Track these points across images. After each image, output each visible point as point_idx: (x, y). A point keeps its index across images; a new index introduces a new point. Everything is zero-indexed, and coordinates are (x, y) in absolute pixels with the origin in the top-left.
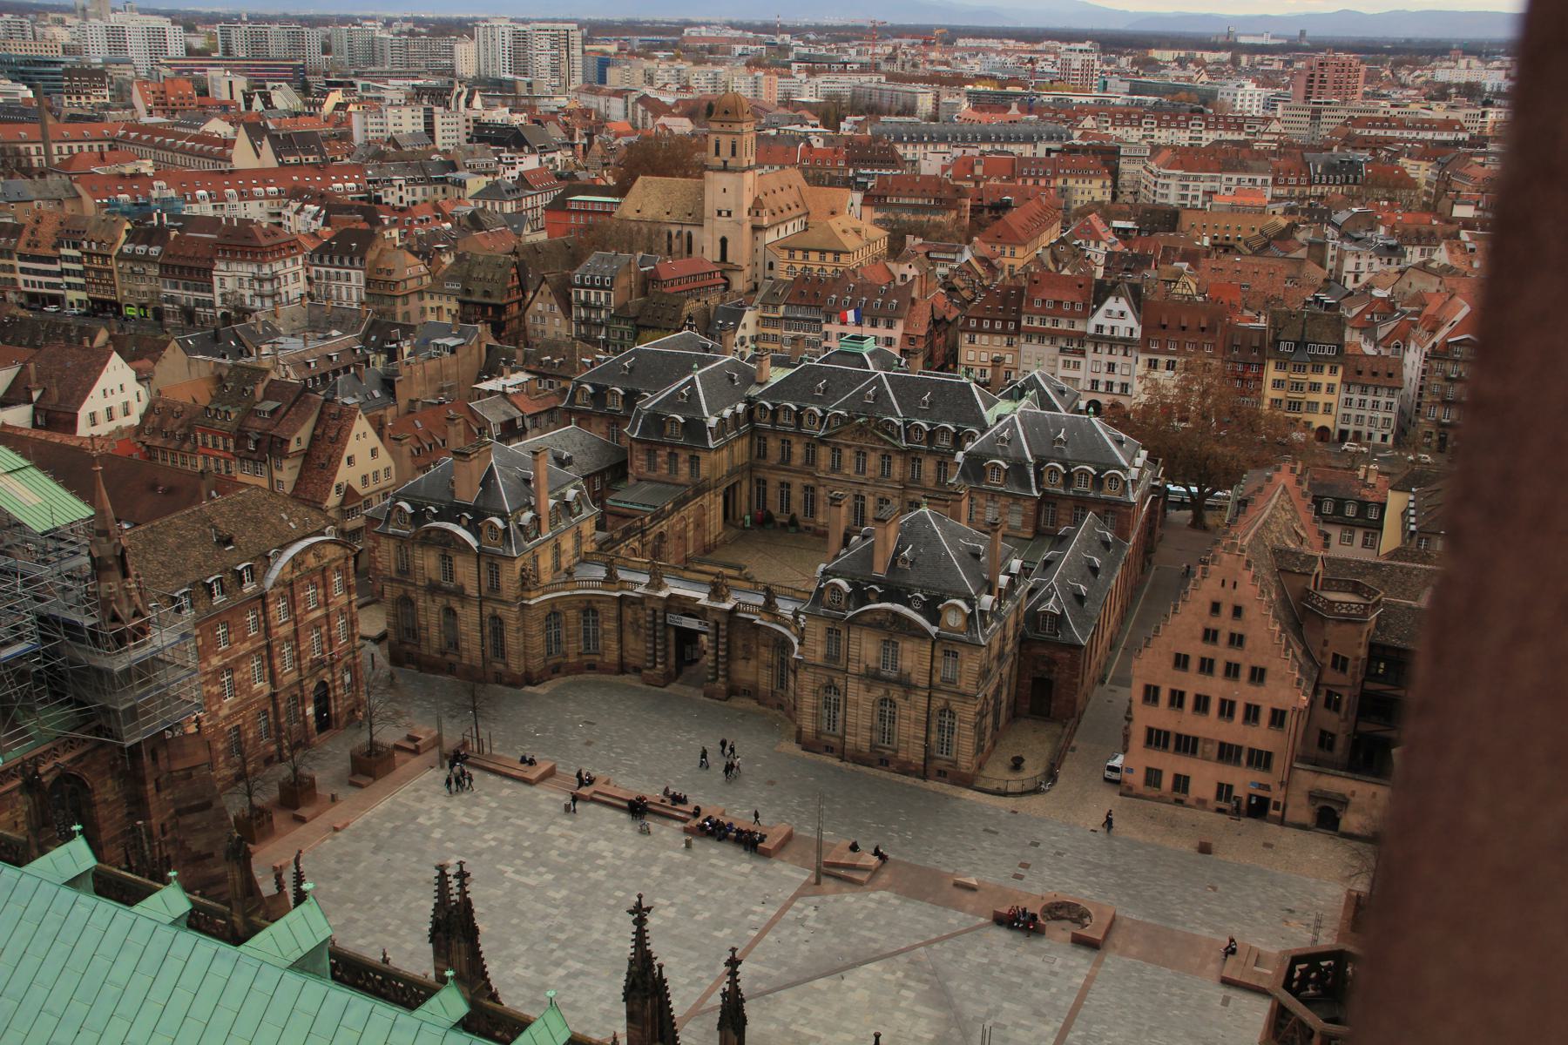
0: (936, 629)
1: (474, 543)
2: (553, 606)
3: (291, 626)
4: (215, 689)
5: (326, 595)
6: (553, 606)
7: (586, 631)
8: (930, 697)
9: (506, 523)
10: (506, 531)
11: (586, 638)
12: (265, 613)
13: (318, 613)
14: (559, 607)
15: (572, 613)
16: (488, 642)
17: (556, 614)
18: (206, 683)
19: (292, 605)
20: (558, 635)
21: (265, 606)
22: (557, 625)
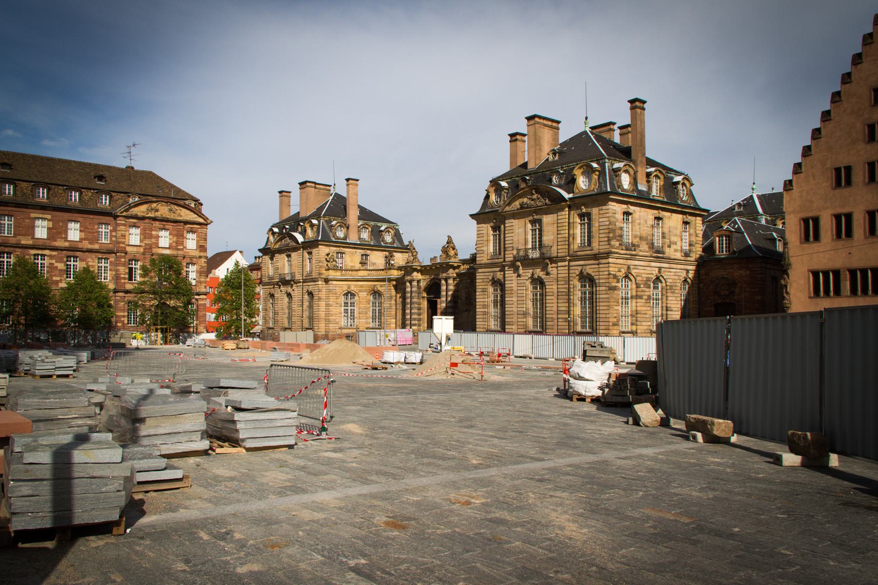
0: (571, 196)
1: (300, 238)
2: (349, 287)
3: (142, 250)
4: (61, 266)
5: (177, 243)
6: (349, 287)
7: (374, 311)
8: (569, 266)
9: (319, 222)
10: (319, 226)
11: (374, 319)
12: (115, 230)
13: (167, 252)
14: (352, 288)
15: (363, 295)
16: (306, 314)
17: (353, 295)
18: (51, 257)
19: (145, 236)
20: (353, 312)
21: (118, 225)
22: (352, 304)
